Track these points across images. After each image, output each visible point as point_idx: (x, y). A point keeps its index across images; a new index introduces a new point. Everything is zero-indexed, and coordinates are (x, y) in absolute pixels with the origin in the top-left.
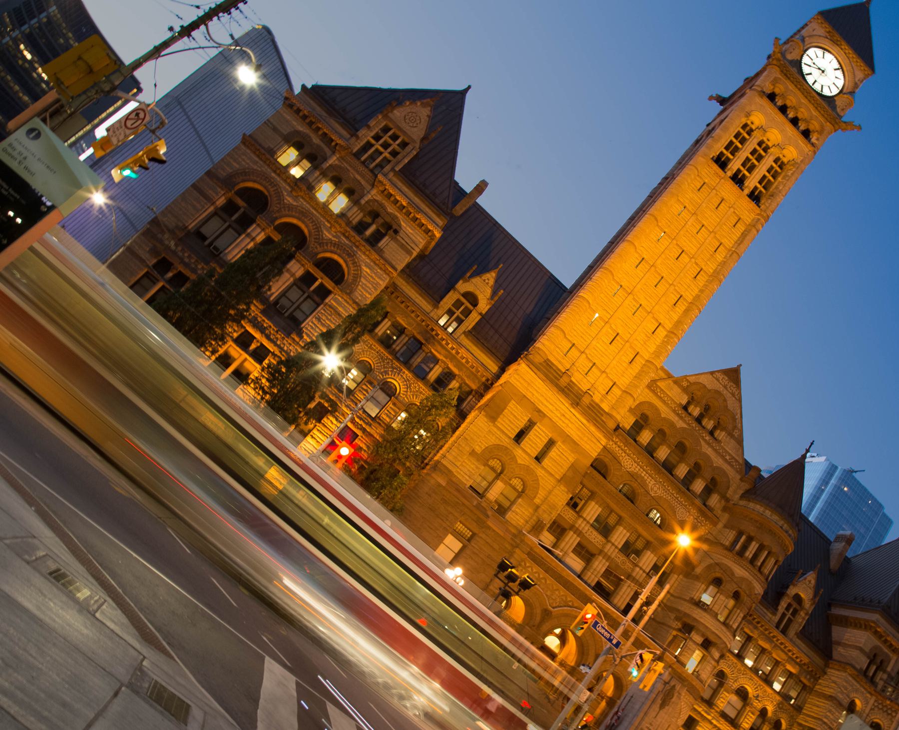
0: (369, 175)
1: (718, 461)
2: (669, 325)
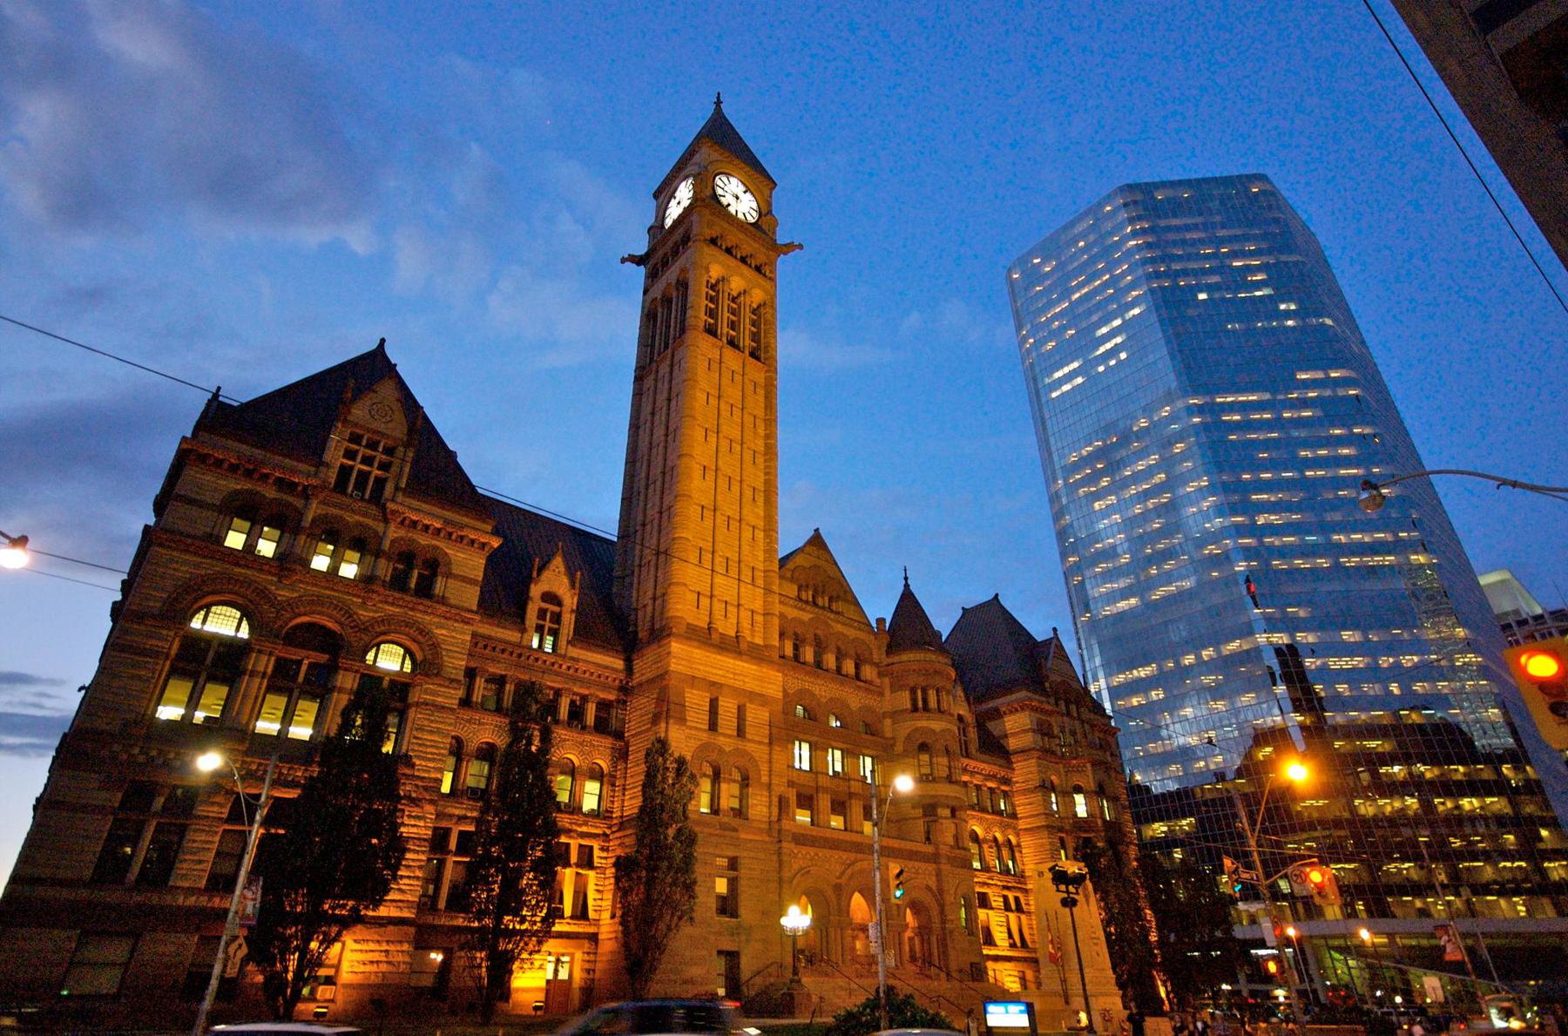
0: (373, 510)
1: (852, 633)
2: (761, 524)
